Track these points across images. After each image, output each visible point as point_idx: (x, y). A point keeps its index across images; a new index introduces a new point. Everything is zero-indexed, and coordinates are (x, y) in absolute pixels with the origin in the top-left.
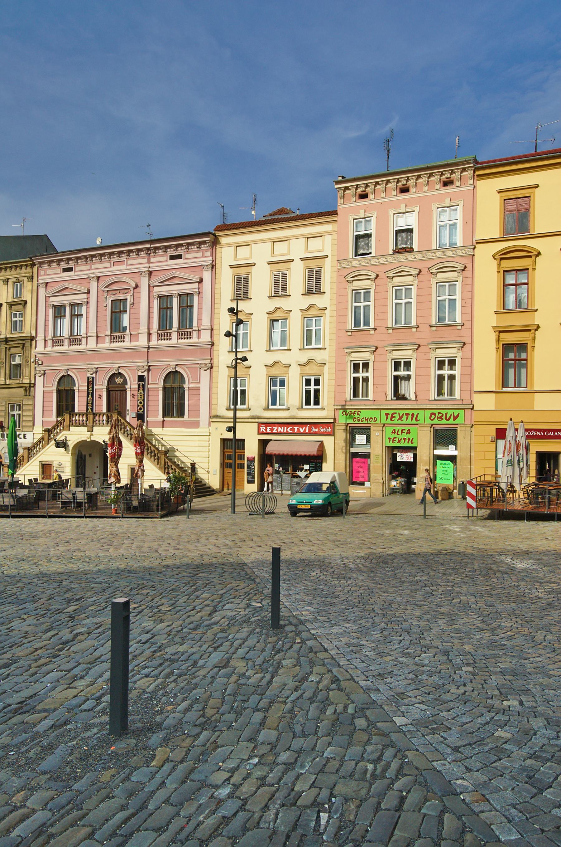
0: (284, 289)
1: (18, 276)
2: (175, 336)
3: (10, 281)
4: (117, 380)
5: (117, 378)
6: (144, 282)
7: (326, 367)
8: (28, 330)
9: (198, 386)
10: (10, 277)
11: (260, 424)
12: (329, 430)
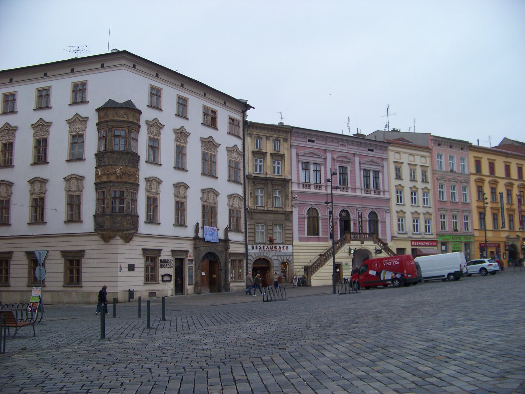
0: (414, 177)
1: (277, 136)
2: (372, 192)
3: (271, 138)
4: (342, 214)
5: (343, 213)
6: (357, 159)
7: (432, 215)
8: (286, 175)
9: (385, 220)
10: (272, 135)
11: (412, 241)
12: (435, 244)
